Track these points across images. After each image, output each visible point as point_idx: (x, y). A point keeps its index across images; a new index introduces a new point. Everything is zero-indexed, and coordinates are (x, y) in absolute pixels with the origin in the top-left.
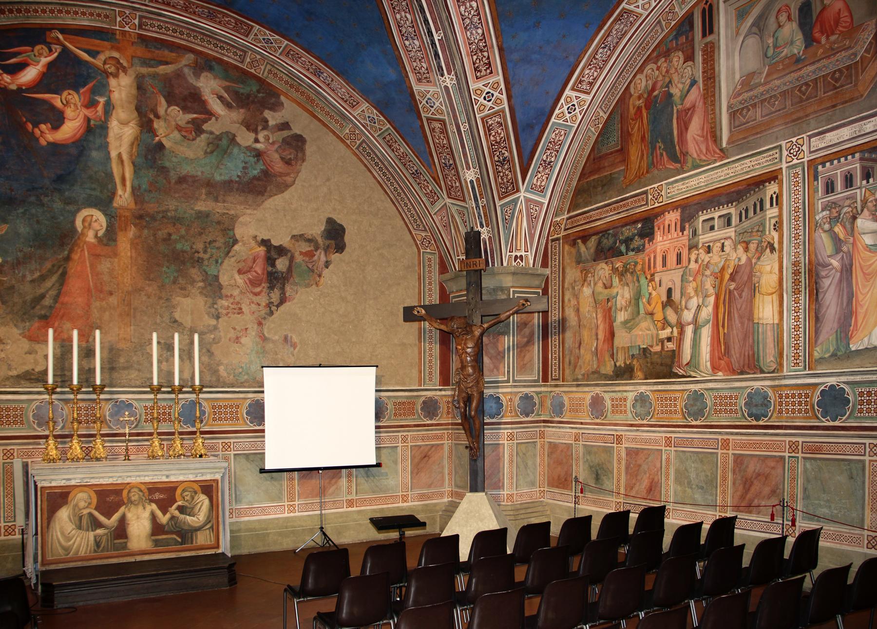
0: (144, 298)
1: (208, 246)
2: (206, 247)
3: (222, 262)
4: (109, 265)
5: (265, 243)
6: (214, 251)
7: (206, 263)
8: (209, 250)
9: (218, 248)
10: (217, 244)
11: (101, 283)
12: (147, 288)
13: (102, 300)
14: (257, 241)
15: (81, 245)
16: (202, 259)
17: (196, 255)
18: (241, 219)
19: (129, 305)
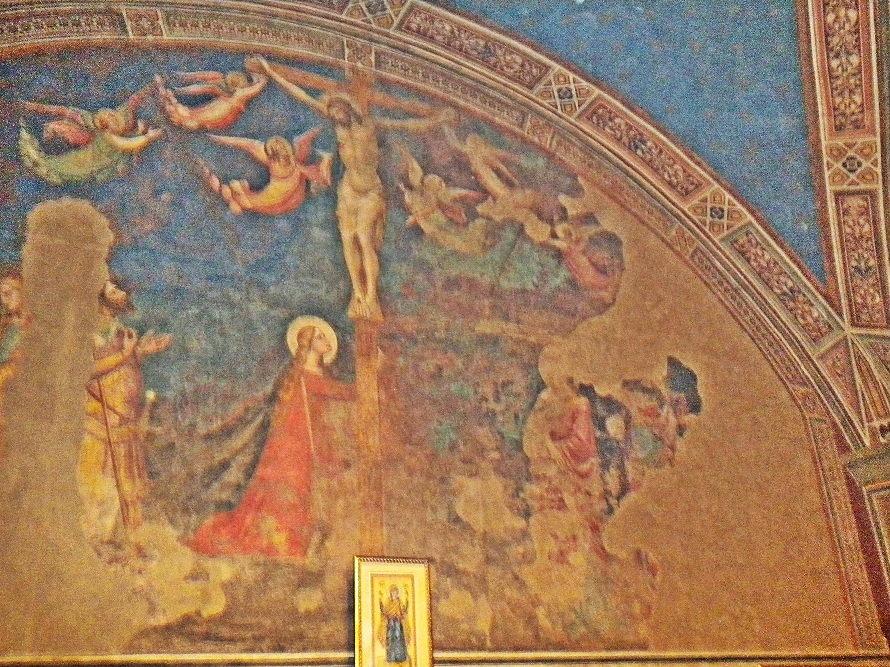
0: (404, 475)
1: (500, 390)
2: (497, 391)
3: (525, 418)
4: (341, 413)
5: (586, 390)
6: (511, 399)
7: (500, 418)
8: (503, 397)
9: (518, 395)
10: (514, 389)
11: (330, 447)
12: (407, 458)
13: (331, 475)
14: (573, 388)
15: (296, 376)
16: (494, 413)
17: (484, 404)
18: (547, 350)
19: (379, 487)
